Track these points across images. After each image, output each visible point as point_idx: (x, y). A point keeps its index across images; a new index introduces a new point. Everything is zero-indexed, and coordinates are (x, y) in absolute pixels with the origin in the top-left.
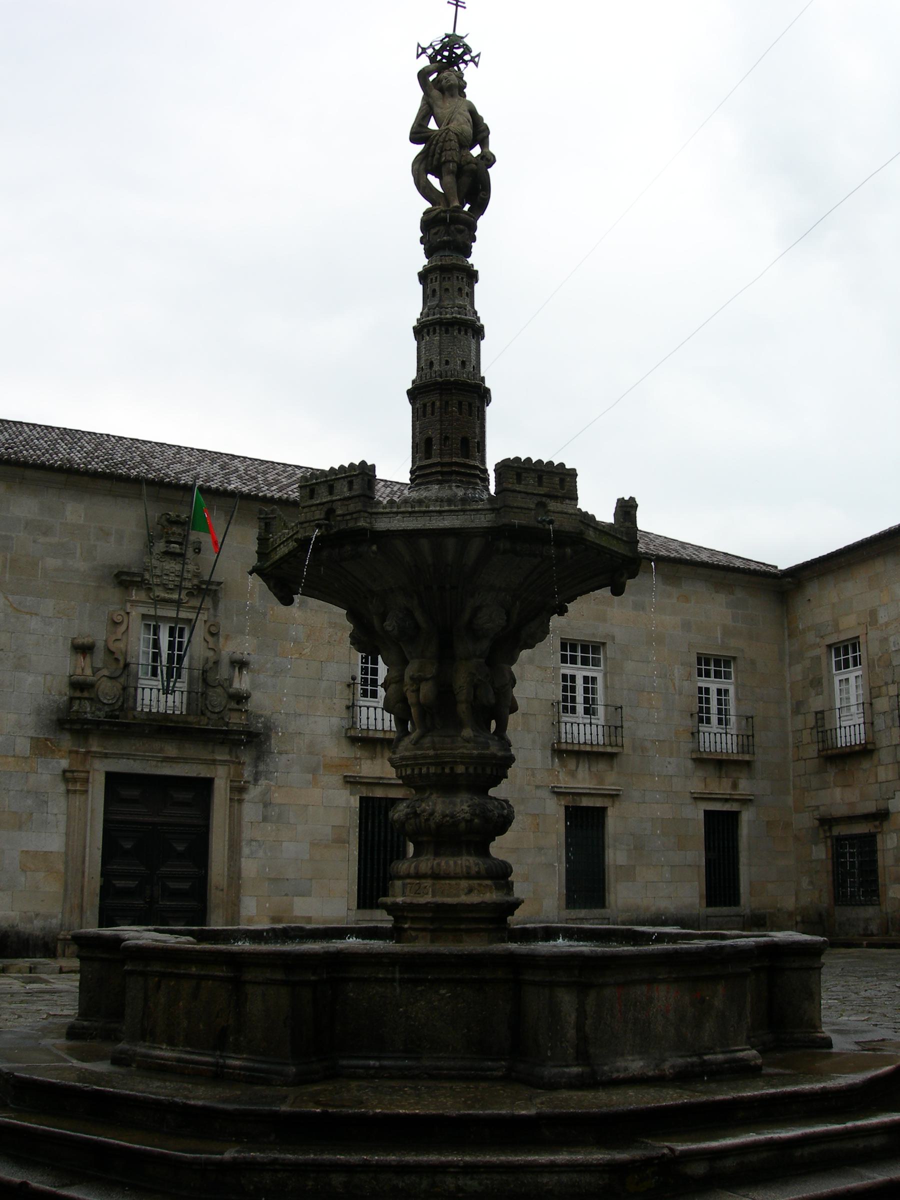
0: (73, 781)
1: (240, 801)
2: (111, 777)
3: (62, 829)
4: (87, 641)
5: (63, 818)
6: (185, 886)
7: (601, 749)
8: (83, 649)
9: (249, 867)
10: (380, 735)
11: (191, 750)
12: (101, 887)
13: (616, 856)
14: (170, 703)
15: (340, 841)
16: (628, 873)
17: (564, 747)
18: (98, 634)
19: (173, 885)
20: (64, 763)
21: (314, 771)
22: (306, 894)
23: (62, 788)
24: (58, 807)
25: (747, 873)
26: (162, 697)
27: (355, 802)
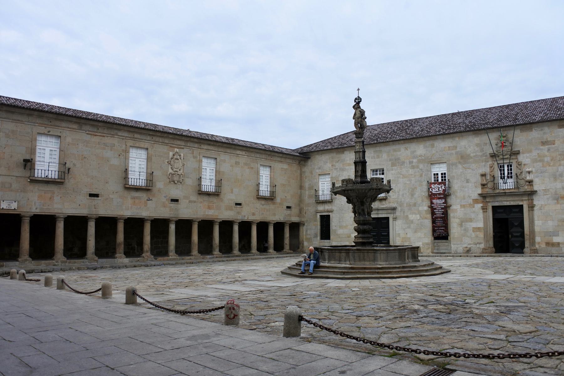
0: (484, 209)
1: (533, 210)
2: (493, 207)
3: (482, 221)
4: (483, 173)
5: (482, 219)
6: (518, 234)
8: (483, 175)
9: (537, 229)
11: (516, 198)
12: (494, 236)
18: (487, 170)
19: (515, 234)
20: (481, 205)
21: (557, 200)
22: (558, 235)
23: (481, 211)
24: (481, 215)
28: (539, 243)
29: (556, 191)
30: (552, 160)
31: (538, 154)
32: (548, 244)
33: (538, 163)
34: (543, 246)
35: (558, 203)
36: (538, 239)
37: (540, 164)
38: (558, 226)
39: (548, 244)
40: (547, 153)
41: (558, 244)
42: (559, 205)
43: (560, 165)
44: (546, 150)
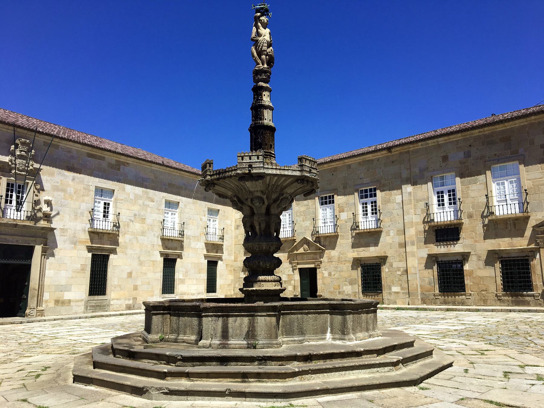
7: (177, 239)
9: (47, 281)
10: (101, 231)
13: (178, 275)
14: (19, 216)
15: (83, 270)
16: (182, 281)
17: (165, 237)
21: (75, 244)
22: (69, 290)
25: (219, 282)
26: (16, 213)
27: (90, 255)
28: (46, 301)
29: (75, 233)
30: (75, 193)
31: (61, 181)
32: (57, 302)
33: (60, 193)
34: (52, 305)
35: (75, 248)
36: (46, 296)
37: (62, 194)
38: (72, 277)
39: (57, 302)
40: (71, 183)
41: (70, 301)
42: (76, 251)
43: (83, 201)
44: (71, 178)
